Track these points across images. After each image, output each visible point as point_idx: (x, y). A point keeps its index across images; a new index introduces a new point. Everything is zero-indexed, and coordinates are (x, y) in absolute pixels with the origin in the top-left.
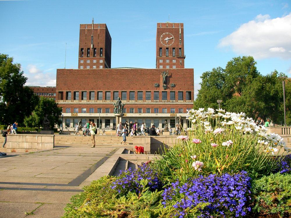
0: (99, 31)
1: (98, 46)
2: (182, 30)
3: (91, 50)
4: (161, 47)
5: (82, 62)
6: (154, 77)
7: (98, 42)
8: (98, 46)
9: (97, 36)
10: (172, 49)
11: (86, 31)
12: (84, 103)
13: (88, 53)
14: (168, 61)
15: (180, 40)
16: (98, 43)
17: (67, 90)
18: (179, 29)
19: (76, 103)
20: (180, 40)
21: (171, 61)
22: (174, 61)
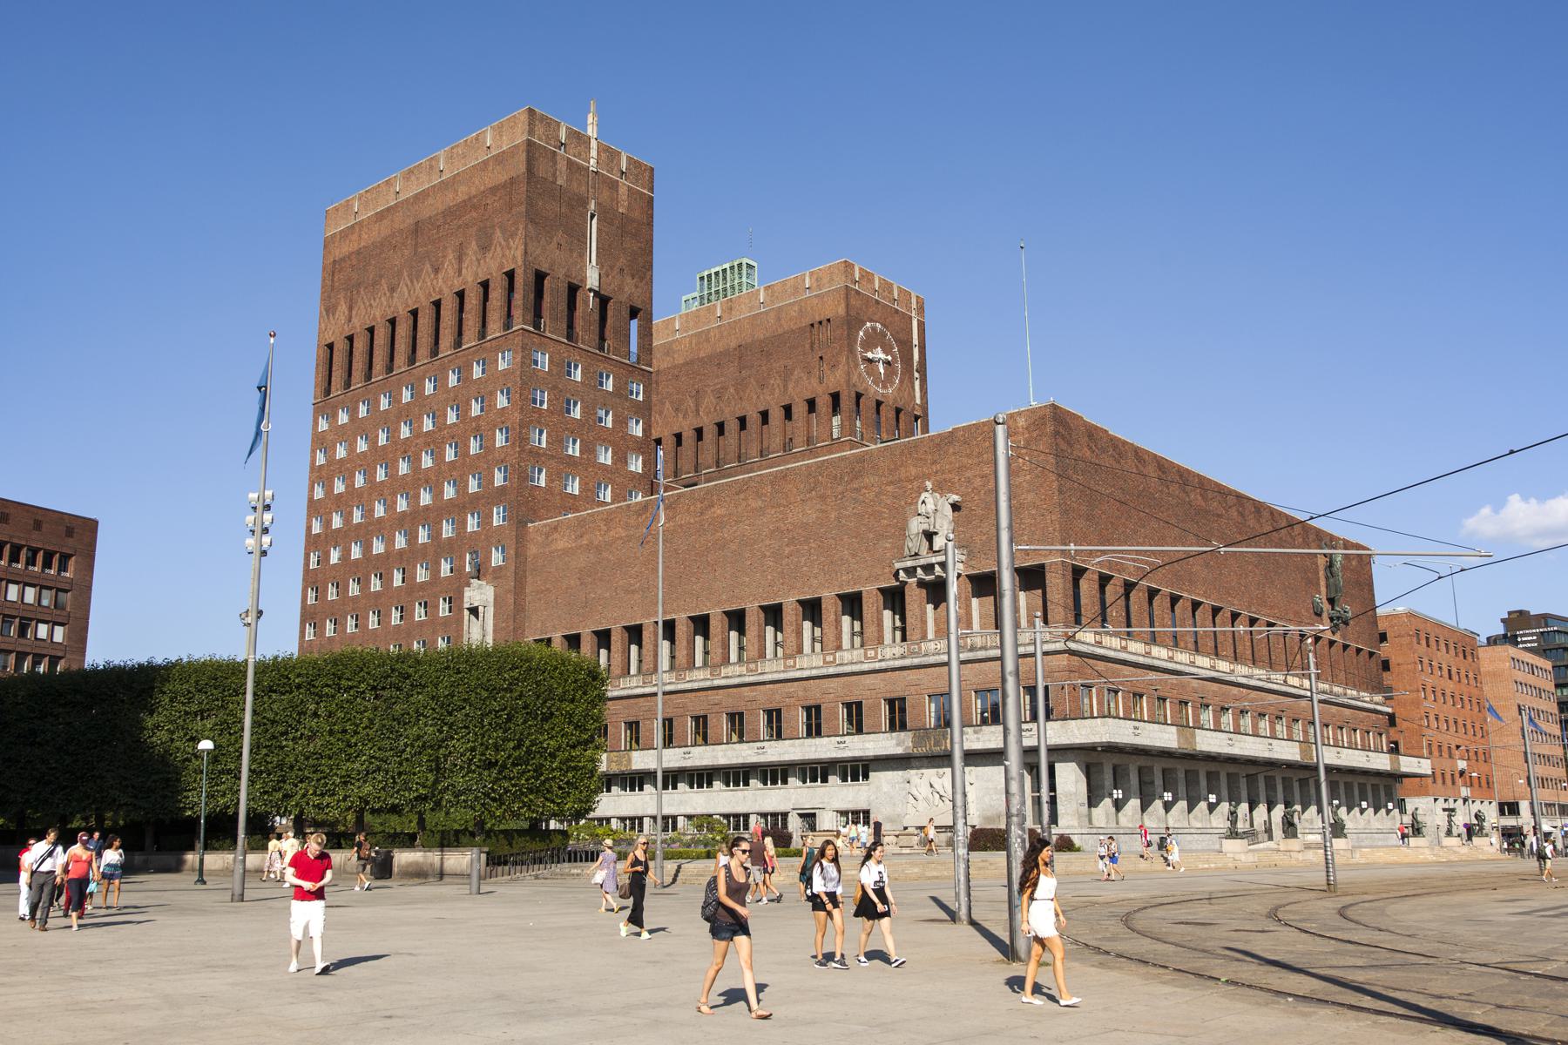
0: (623, 191)
5: (544, 361)
7: (619, 264)
8: (621, 288)
11: (562, 166)
20: (916, 375)
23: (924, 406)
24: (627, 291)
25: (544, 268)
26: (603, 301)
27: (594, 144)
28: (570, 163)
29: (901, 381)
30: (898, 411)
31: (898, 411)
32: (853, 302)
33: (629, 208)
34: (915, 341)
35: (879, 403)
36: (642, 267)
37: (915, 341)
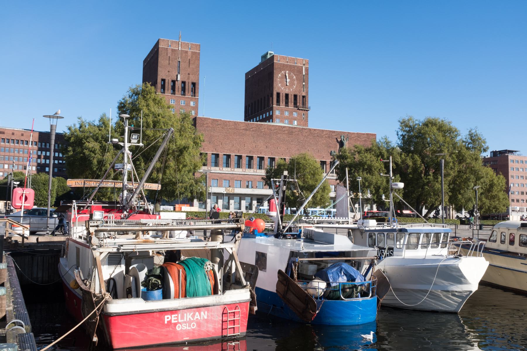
1: (188, 79)
2: (307, 70)
3: (179, 85)
4: (278, 91)
6: (330, 141)
7: (188, 72)
8: (188, 79)
9: (188, 62)
10: (293, 97)
12: (238, 173)
13: (173, 88)
14: (287, 114)
15: (304, 83)
16: (189, 74)
17: (212, 151)
18: (302, 67)
19: (227, 172)
21: (291, 113)
22: (295, 114)
23: (307, 93)
24: (193, 79)
25: (164, 78)
26: (184, 83)
27: (180, 43)
28: (172, 50)
29: (296, 87)
30: (295, 96)
31: (295, 96)
32: (275, 66)
33: (192, 57)
34: (304, 74)
35: (287, 96)
36: (197, 72)
37: (304, 74)
